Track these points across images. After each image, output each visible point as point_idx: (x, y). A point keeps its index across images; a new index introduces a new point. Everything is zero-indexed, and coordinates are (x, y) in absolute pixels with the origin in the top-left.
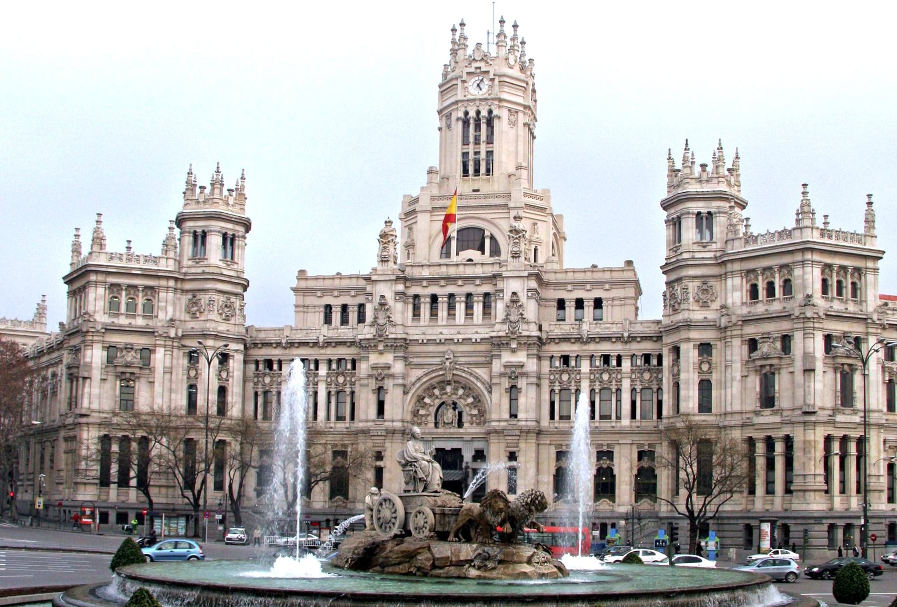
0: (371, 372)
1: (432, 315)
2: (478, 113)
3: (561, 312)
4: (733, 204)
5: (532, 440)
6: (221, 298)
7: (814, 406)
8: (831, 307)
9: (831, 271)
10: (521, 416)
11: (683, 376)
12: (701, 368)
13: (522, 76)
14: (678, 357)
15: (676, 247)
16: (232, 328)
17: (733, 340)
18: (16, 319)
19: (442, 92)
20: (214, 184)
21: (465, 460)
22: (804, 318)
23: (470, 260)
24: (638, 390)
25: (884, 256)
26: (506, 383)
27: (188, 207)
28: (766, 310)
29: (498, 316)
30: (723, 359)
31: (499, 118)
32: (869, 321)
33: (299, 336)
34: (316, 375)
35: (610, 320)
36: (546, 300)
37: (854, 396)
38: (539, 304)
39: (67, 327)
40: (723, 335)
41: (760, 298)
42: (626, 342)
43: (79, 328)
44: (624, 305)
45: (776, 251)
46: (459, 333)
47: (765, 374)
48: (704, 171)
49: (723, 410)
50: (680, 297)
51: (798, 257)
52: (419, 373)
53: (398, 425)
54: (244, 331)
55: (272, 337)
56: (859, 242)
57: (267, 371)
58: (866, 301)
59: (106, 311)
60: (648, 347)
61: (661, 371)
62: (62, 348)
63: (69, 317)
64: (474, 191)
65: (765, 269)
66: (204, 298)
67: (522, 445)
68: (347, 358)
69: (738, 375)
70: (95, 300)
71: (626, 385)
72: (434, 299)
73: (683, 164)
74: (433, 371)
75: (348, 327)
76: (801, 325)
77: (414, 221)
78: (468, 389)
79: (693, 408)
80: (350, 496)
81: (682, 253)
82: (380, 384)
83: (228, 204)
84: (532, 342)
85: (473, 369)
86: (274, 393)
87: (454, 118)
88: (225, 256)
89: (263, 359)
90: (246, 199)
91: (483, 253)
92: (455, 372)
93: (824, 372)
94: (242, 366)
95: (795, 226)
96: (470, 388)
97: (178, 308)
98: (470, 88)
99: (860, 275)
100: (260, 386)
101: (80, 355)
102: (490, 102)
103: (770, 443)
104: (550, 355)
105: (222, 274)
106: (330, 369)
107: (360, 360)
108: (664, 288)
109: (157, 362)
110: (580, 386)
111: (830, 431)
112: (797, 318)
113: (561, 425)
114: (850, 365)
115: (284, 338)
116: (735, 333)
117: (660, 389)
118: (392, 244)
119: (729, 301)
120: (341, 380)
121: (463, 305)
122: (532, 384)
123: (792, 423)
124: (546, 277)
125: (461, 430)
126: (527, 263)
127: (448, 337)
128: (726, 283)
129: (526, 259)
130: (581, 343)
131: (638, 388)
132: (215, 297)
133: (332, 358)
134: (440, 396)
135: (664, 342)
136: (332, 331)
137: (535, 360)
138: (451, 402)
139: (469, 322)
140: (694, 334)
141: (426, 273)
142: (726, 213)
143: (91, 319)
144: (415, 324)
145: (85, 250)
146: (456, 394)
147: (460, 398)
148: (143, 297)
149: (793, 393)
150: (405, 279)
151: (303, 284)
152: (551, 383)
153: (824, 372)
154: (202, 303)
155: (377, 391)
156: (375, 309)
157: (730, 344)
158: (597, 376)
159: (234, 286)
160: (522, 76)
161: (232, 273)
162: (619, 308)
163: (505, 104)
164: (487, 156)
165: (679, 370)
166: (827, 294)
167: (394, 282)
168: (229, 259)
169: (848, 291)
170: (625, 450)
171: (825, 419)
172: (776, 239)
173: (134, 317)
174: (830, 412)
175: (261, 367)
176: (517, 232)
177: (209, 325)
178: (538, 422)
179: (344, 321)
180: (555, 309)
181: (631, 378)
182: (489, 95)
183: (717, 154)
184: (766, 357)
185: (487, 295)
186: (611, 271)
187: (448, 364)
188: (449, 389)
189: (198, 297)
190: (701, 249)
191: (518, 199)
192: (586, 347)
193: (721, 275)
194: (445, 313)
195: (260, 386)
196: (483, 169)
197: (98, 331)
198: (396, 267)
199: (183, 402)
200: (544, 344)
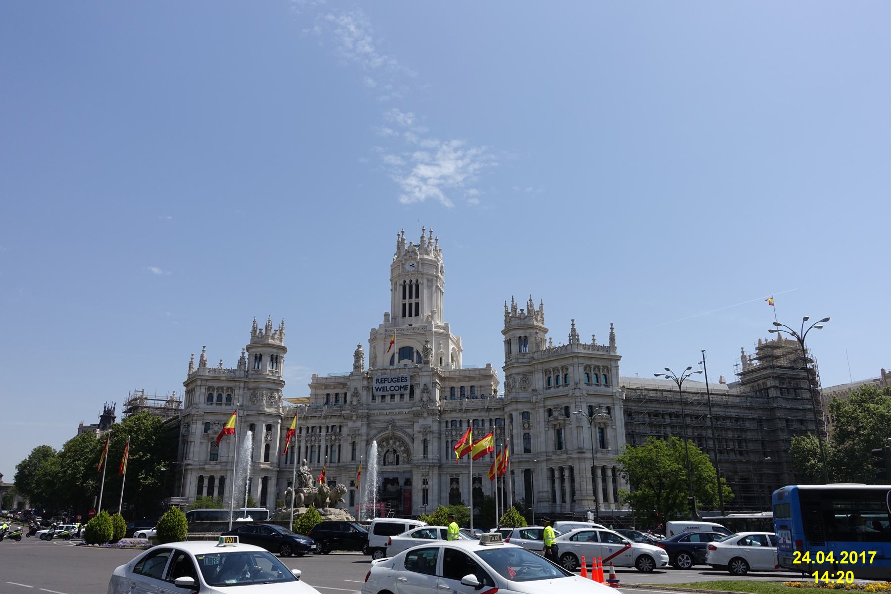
5: (436, 471)
10: (430, 456)
11: (515, 431)
17: (540, 409)
26: (421, 438)
34: (320, 436)
49: (537, 451)
58: (612, 385)
79: (521, 450)
87: (398, 284)
96: (402, 441)
98: (407, 267)
106: (328, 432)
114: (604, 424)
120: (333, 438)
138: (391, 450)
140: (520, 406)
184: (556, 419)
187: (390, 427)
188: (391, 442)
190: (521, 357)
193: (532, 372)
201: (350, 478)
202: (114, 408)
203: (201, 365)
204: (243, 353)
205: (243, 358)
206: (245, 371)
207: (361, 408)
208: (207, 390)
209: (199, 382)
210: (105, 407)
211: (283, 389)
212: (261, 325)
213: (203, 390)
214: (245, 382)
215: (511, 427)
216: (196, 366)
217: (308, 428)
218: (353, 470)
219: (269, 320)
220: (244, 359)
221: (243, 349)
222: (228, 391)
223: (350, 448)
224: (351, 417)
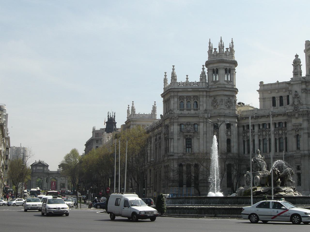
16: (231, 111)
33: (261, 113)
34: (270, 131)
39: (163, 116)
75: (282, 107)
89: (246, 125)
106: (275, 127)
115: (254, 114)
118: (299, 66)
120: (280, 132)
132: (224, 98)
136: (275, 109)
143: (173, 113)
156: (293, 98)
167: (301, 84)
173: (190, 110)
177: (221, 111)
197: (175, 118)
201: (296, 163)
202: (115, 116)
203: (173, 80)
204: (203, 69)
205: (203, 73)
206: (206, 83)
207: (301, 107)
208: (178, 99)
209: (172, 94)
210: (108, 116)
211: (237, 95)
212: (216, 46)
213: (176, 99)
214: (206, 91)
216: (169, 82)
217: (259, 125)
218: (298, 157)
219: (221, 41)
220: (205, 73)
221: (203, 66)
222: (194, 100)
223: (294, 140)
224: (294, 115)
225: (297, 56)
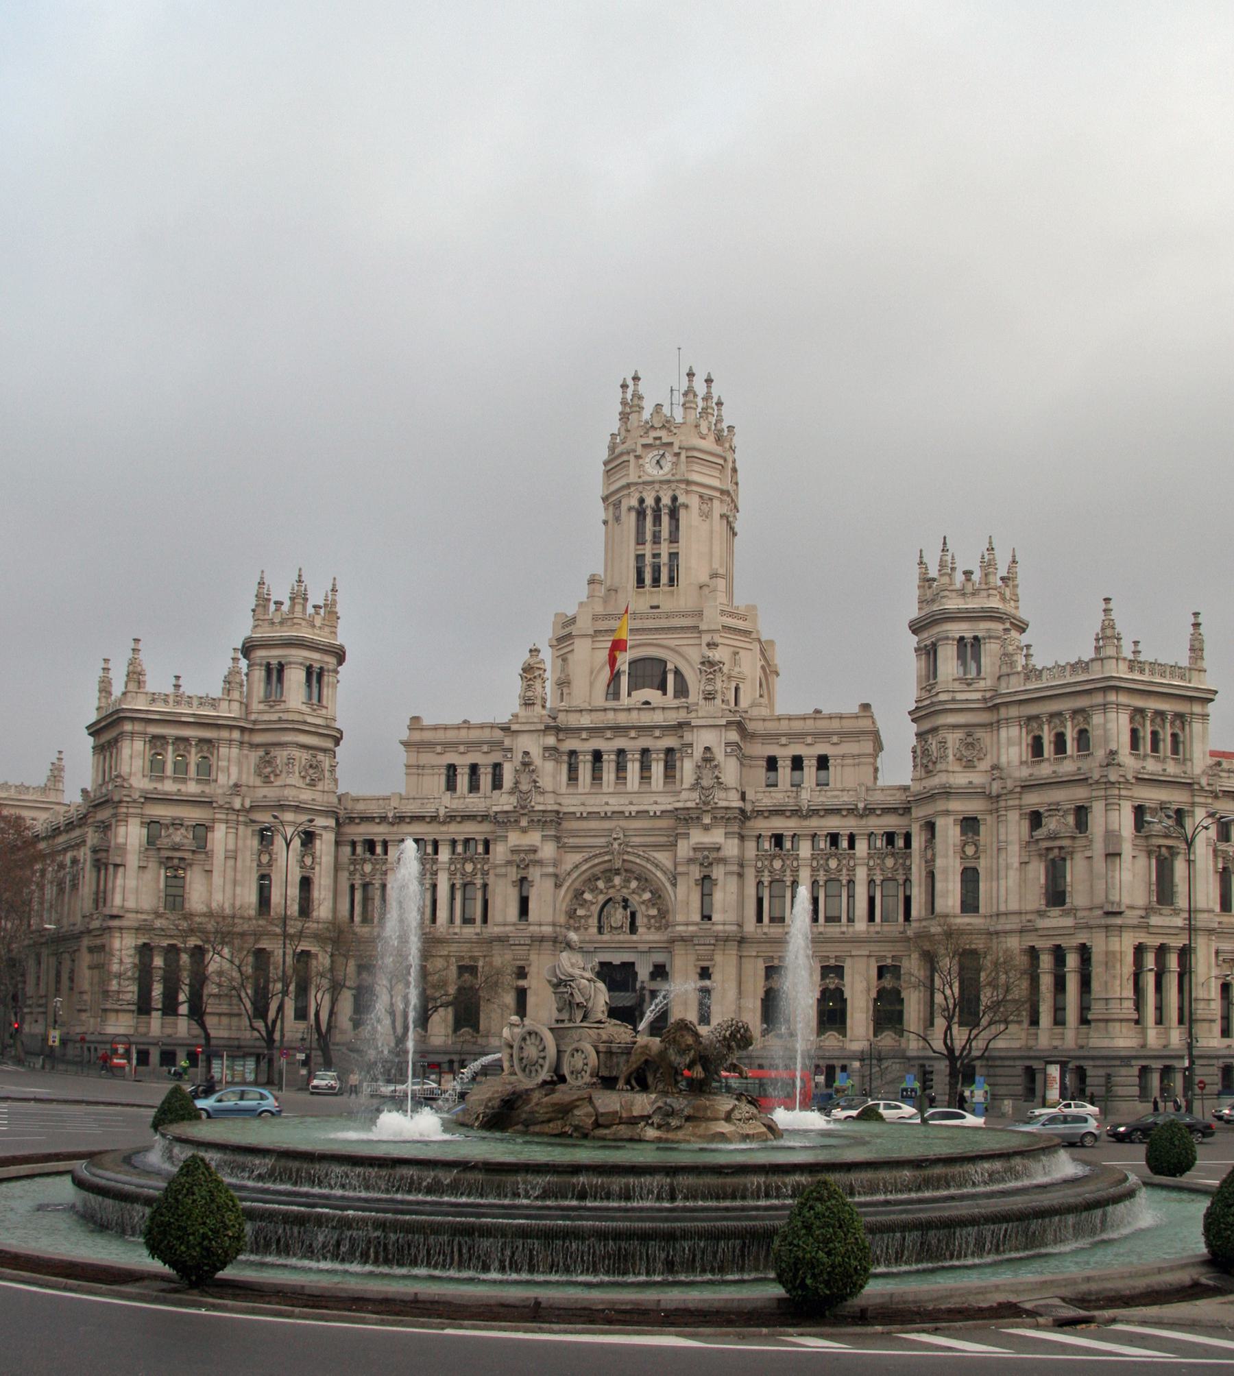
0: (510, 857)
1: (594, 779)
2: (658, 500)
3: (772, 774)
4: (1008, 625)
5: (732, 951)
6: (304, 756)
7: (1119, 904)
8: (1144, 768)
9: (1143, 718)
10: (716, 917)
11: (939, 862)
12: (964, 852)
13: (718, 449)
14: (933, 836)
15: (930, 685)
16: (319, 797)
18: (22, 785)
19: (608, 471)
20: (294, 598)
21: (640, 978)
22: (1105, 783)
23: (647, 703)
24: (878, 882)
25: (1217, 697)
26: (696, 872)
27: (259, 629)
28: (1054, 772)
29: (685, 780)
30: (995, 839)
31: (687, 507)
32: (1196, 787)
33: (411, 808)
34: (435, 861)
35: (839, 786)
36: (751, 758)
37: (1175, 889)
38: (741, 764)
40: (995, 806)
41: (1046, 755)
42: (862, 816)
43: (109, 797)
44: (859, 765)
45: (1068, 690)
46: (631, 803)
47: (1053, 860)
48: (968, 580)
50: (935, 754)
51: (1098, 699)
52: (577, 858)
53: (547, 930)
54: (335, 800)
55: (374, 809)
56: (1182, 678)
57: (368, 855)
58: (1191, 760)
59: (146, 773)
60: (891, 822)
61: (909, 856)
62: (85, 824)
63: (95, 781)
64: (652, 607)
65: (1052, 716)
66: (281, 755)
67: (718, 958)
68: (477, 838)
69: (1015, 861)
70: (131, 757)
71: (861, 874)
72: (597, 756)
73: (940, 571)
74: (596, 856)
75: (479, 795)
76: (1102, 793)
77: (569, 649)
78: (644, 880)
80: (482, 1027)
81: (938, 693)
82: (523, 873)
83: (314, 626)
84: (732, 816)
85: (651, 853)
86: (377, 886)
87: (624, 507)
88: (310, 698)
89: (361, 839)
90: (338, 618)
91: (665, 693)
92: (626, 857)
93: (1134, 857)
94: (333, 848)
95: (1093, 656)
96: (646, 879)
97: (245, 769)
98: (647, 466)
99: (1183, 723)
100: (358, 876)
101: (111, 834)
102: (673, 486)
103: (1059, 954)
104: (757, 833)
105: (305, 722)
106: (453, 852)
107: (495, 840)
108: (913, 741)
109: (216, 843)
110: (798, 876)
111: (1143, 938)
112: (1097, 782)
113: (772, 930)
114: (1169, 848)
115: (390, 810)
116: (1010, 803)
117: (907, 881)
118: (539, 681)
119: (1004, 759)
120: (469, 867)
121: (637, 765)
122: (731, 873)
123: (1089, 927)
124: (751, 726)
125: (634, 937)
126: (724, 707)
127: (616, 809)
128: (998, 734)
129: (723, 701)
130: (800, 817)
131: (878, 879)
132: (297, 753)
133: (456, 838)
134: (605, 891)
135: (914, 815)
136: (457, 801)
137: (736, 841)
138: (621, 898)
139: (645, 788)
140: (955, 805)
141: (585, 721)
142: (998, 638)
143: (126, 785)
144: (571, 790)
145: (117, 689)
146: (628, 888)
147: (633, 892)
148: (196, 755)
149: (1091, 886)
150: (558, 730)
151: (417, 736)
152: (758, 872)
153: (1134, 857)
154: (278, 762)
155: (518, 883)
156: (516, 771)
157: (1004, 818)
158: (821, 862)
159: (321, 739)
160: (718, 449)
161: (319, 721)
162: (852, 768)
163: (694, 488)
164: (670, 560)
165: (934, 855)
166: (1137, 750)
167: (542, 734)
168: (315, 701)
169: (1166, 746)
170: (861, 965)
171: (1135, 922)
172: (1067, 673)
173: (184, 781)
174: (1142, 913)
175: (359, 850)
176: (711, 664)
177: (289, 793)
178: (740, 925)
179: (474, 787)
180: (764, 770)
181: (868, 865)
182: (673, 475)
183: (987, 557)
184: (1053, 837)
185: (669, 751)
186: (841, 718)
187: (616, 845)
188: (617, 880)
189: (272, 754)
190: (964, 687)
191: (713, 619)
192: (806, 823)
193: (992, 724)
194: (613, 776)
195: (358, 876)
196: (664, 578)
197: (134, 801)
198: (544, 712)
199: (252, 898)
200: (749, 818)
215: (929, 853)
225: (534, 651)
